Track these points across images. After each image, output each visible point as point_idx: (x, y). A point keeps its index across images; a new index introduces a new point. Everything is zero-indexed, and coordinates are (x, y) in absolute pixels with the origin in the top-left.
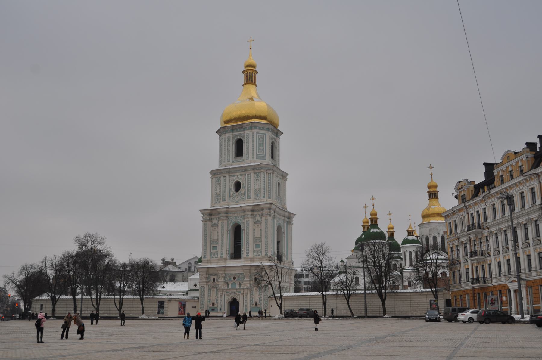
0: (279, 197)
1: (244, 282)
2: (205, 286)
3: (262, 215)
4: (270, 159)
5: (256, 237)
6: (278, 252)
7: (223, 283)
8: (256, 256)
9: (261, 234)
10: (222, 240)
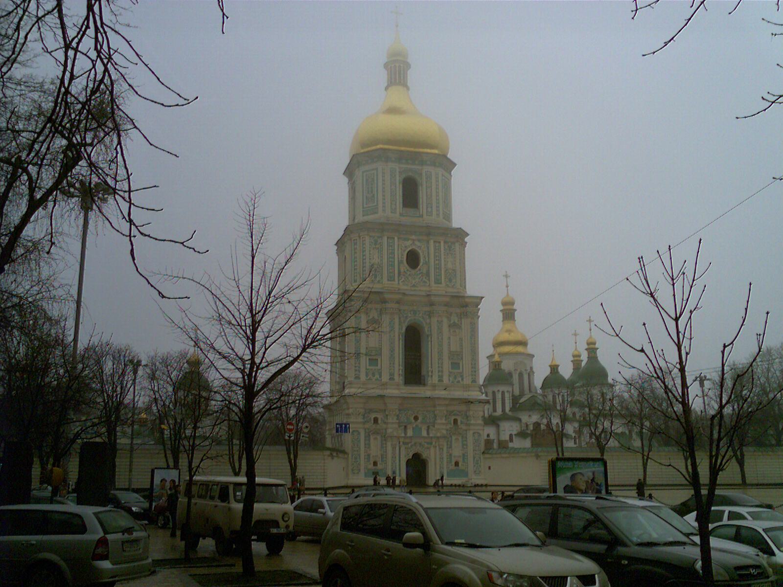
1: (436, 426)
5: (452, 350)
7: (396, 426)
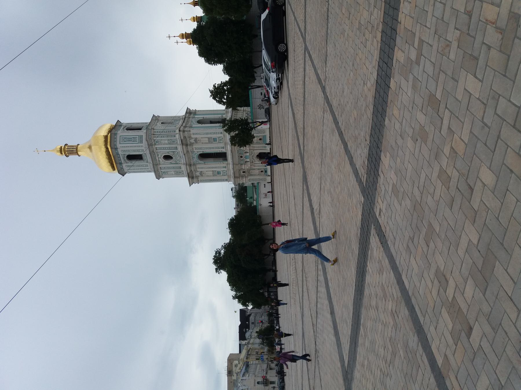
0: (174, 123)
2: (249, 178)
3: (190, 137)
4: (141, 131)
5: (208, 142)
6: (219, 122)
7: (246, 166)
8: (223, 141)
9: (205, 138)
10: (213, 168)
